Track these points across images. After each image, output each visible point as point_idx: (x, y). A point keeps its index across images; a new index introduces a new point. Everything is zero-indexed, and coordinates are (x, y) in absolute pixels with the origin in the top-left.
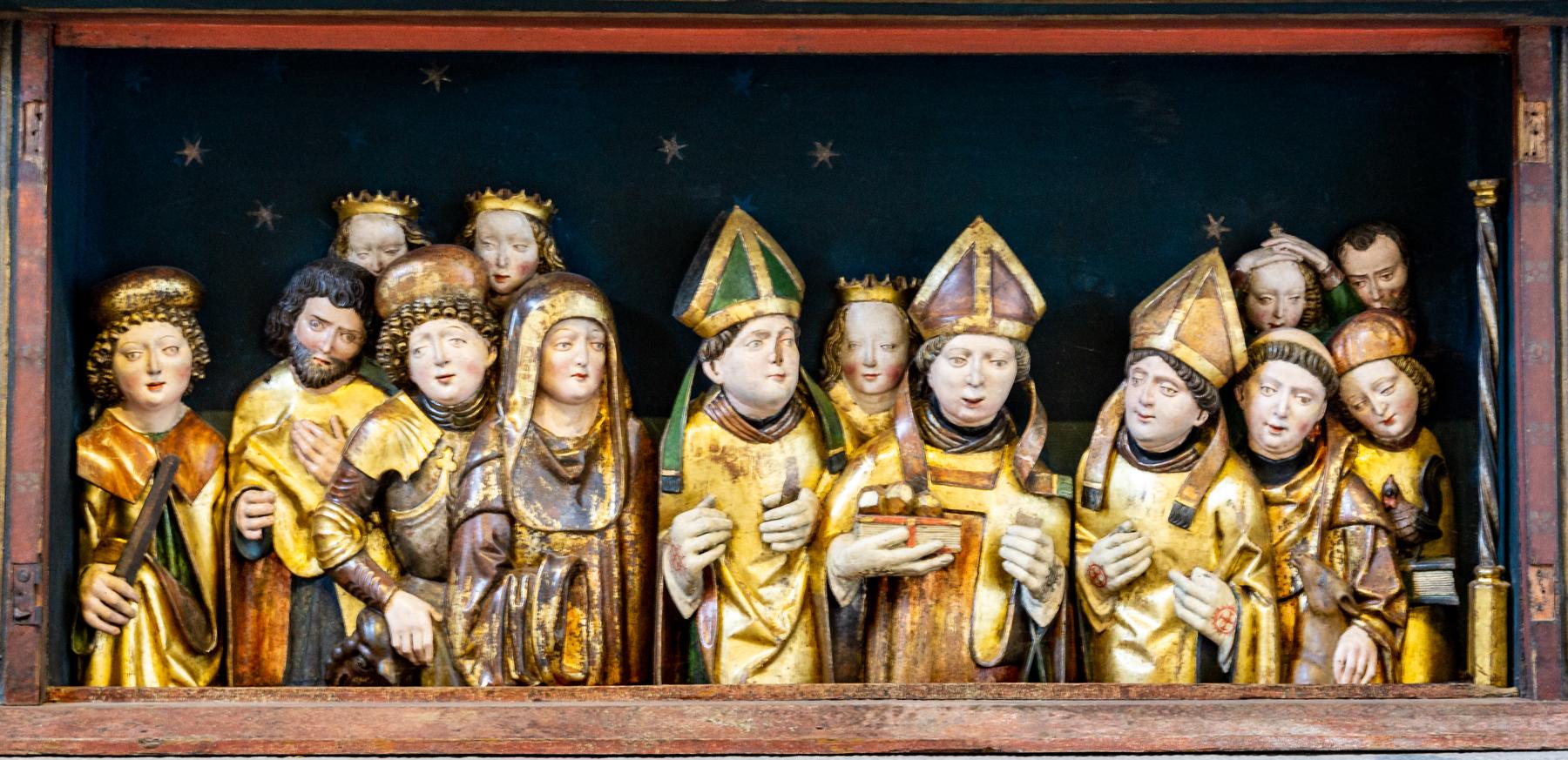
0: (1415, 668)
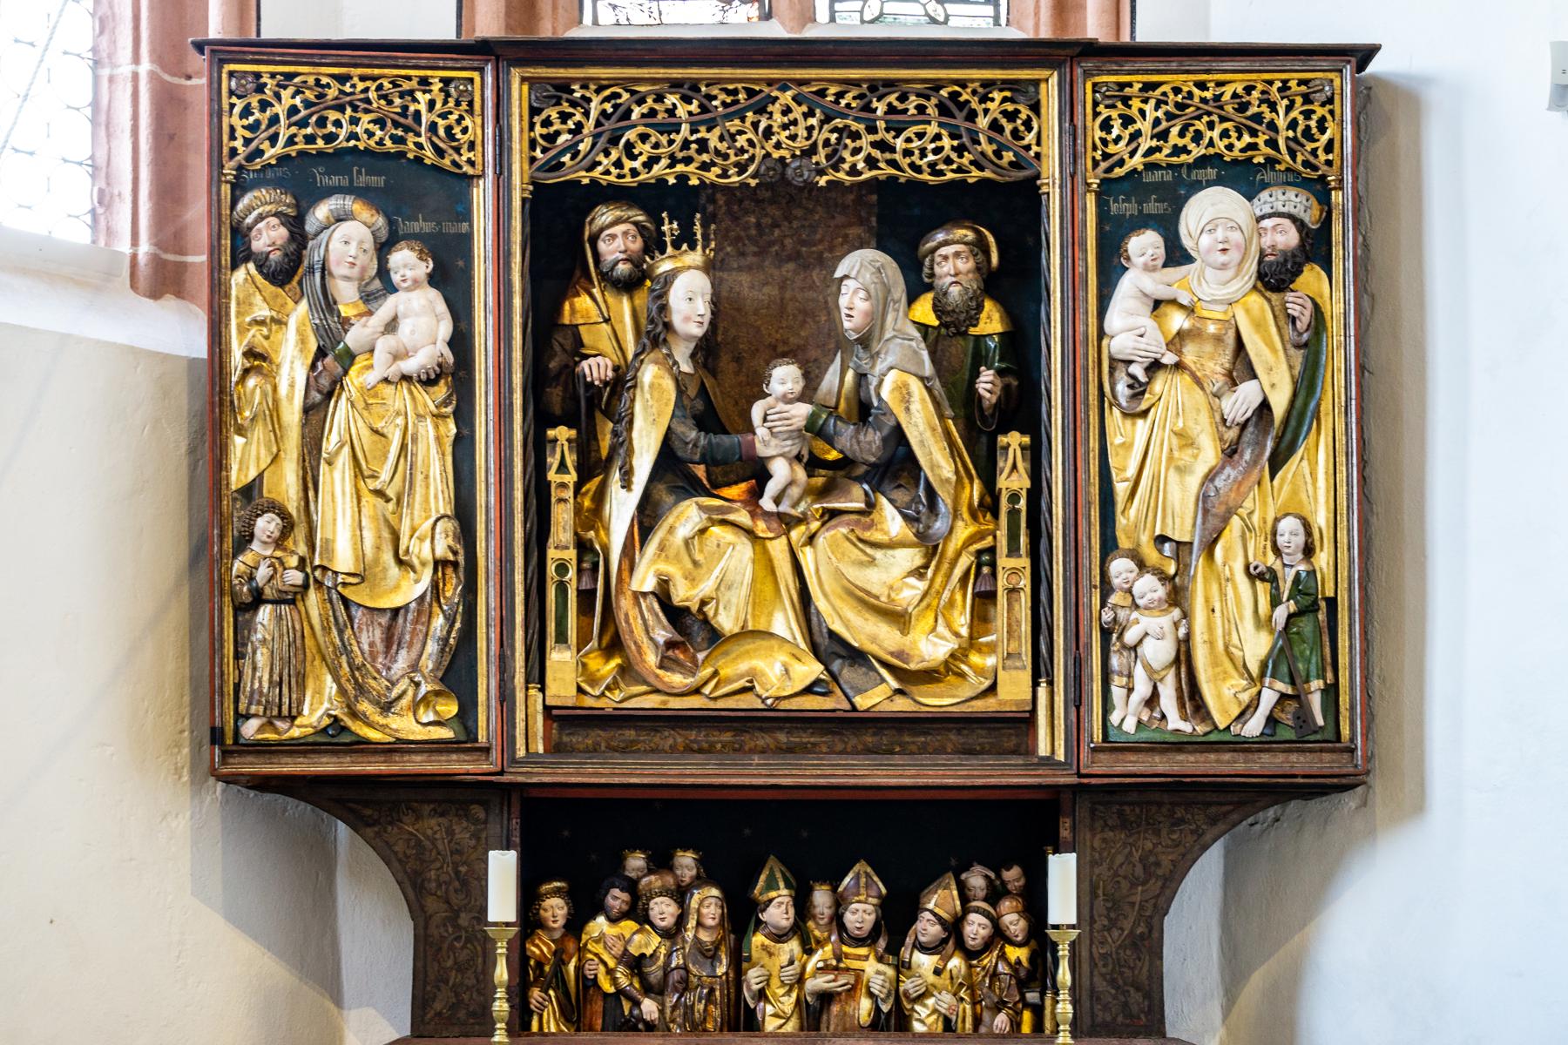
0: (1026, 1028)
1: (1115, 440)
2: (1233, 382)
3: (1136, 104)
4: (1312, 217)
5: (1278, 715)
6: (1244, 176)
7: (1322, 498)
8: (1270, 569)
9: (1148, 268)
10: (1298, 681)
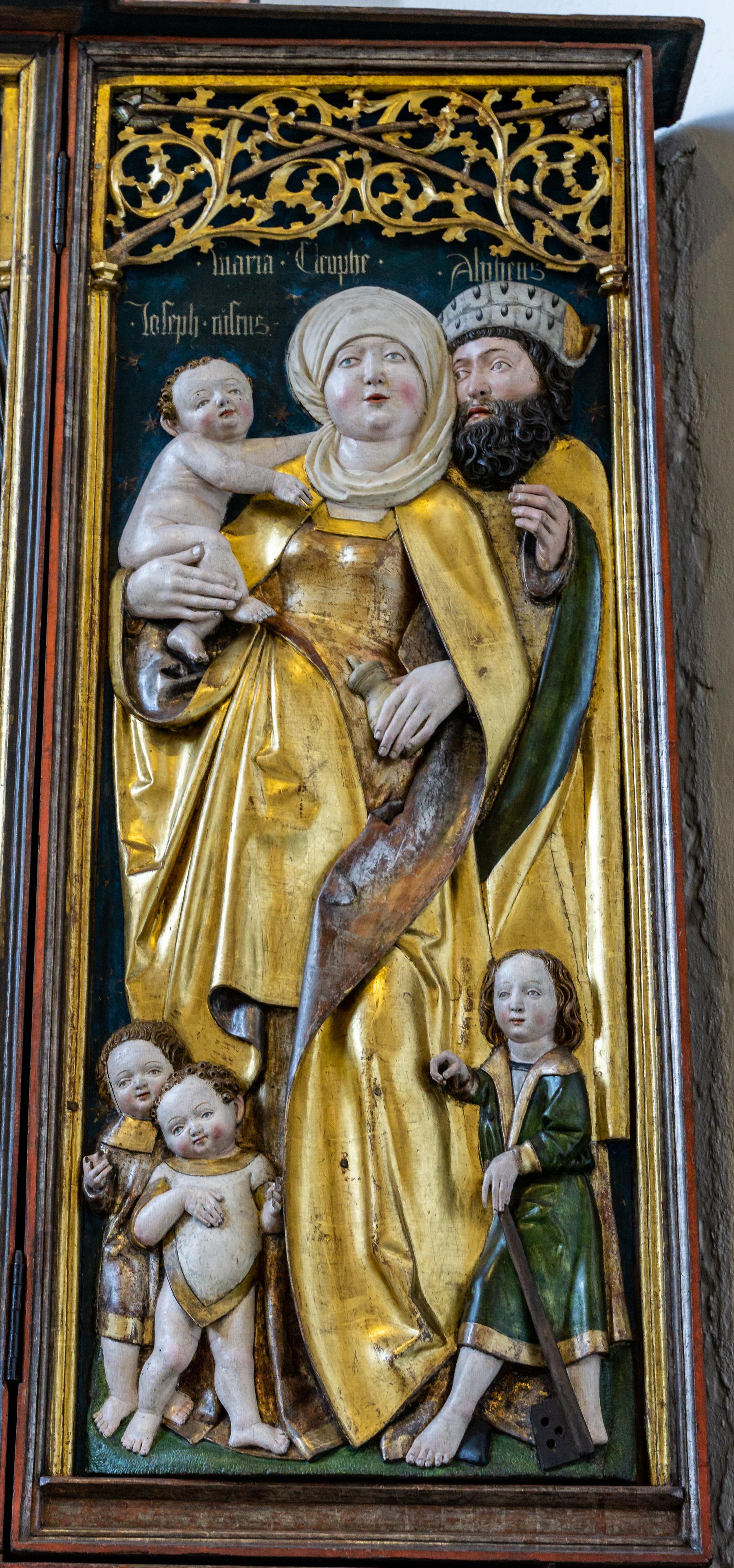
1: (133, 786)
2: (394, 664)
3: (201, 129)
4: (567, 338)
5: (495, 1414)
6: (425, 267)
7: (596, 920)
8: (478, 1074)
9: (216, 433)
10: (543, 1333)
